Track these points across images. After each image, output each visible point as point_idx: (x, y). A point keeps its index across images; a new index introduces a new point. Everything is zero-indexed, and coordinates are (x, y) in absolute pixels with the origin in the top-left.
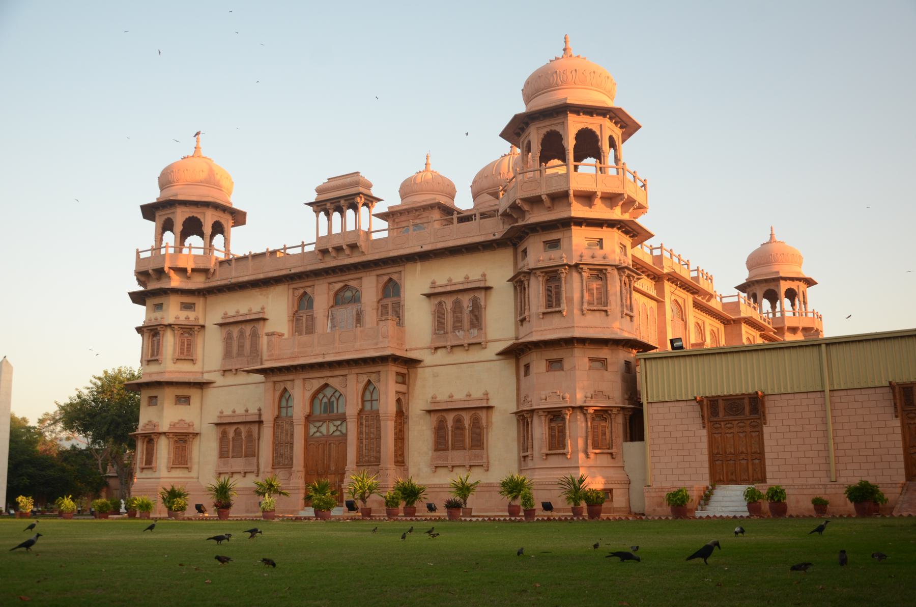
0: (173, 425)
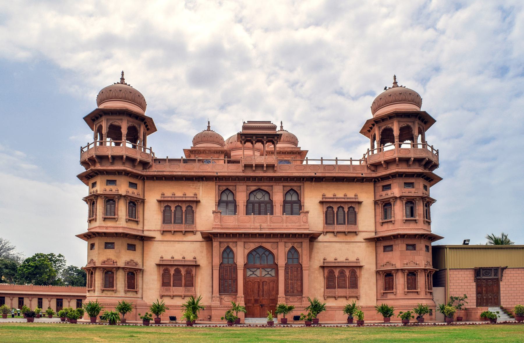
0: (128, 263)
